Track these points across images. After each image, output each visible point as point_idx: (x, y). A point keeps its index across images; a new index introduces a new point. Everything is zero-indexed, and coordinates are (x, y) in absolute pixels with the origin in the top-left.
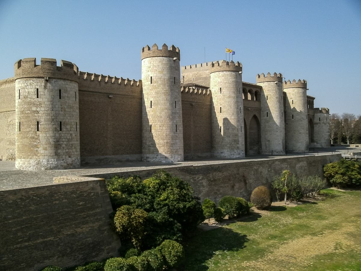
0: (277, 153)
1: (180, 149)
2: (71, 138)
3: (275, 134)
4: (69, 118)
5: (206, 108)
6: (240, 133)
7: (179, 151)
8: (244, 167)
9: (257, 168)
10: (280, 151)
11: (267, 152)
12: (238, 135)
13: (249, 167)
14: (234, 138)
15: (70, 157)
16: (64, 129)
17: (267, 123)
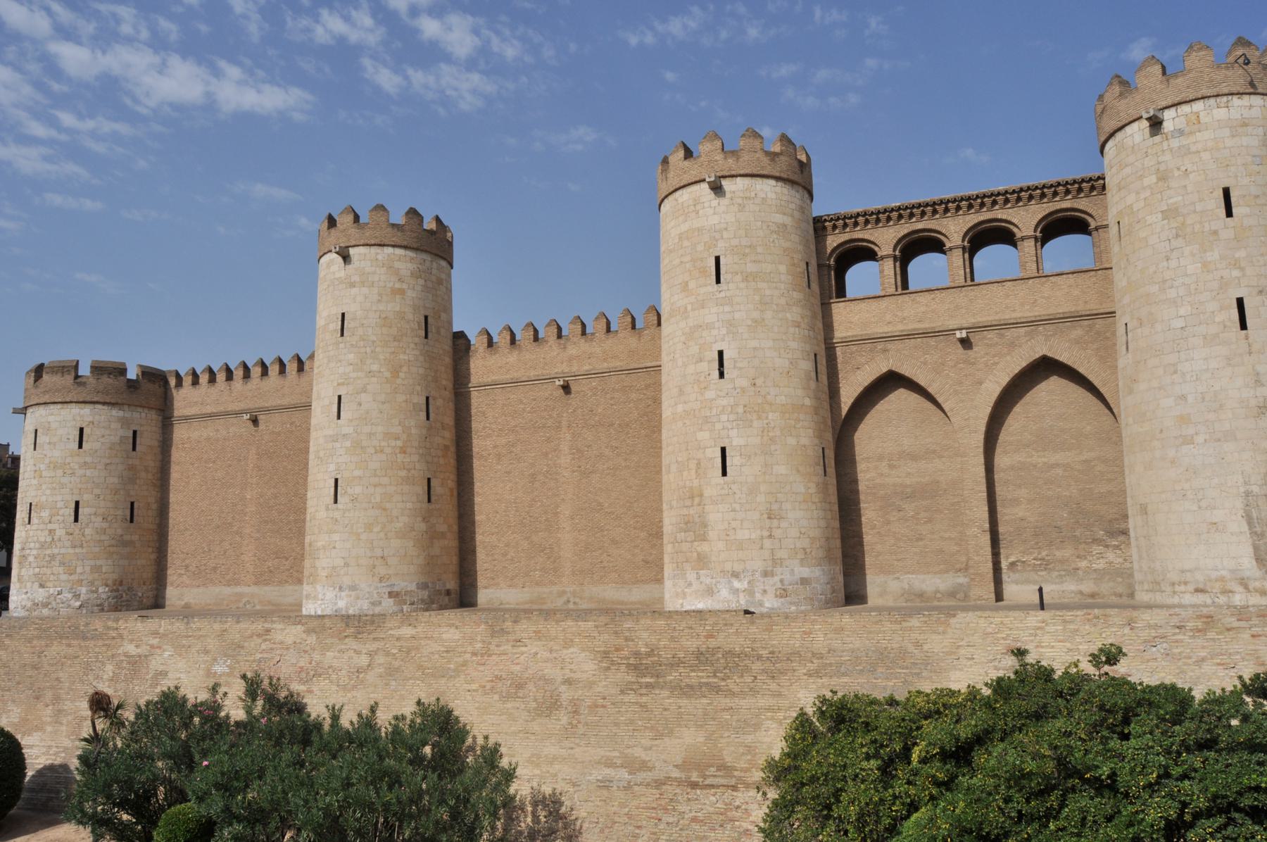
0: (1197, 590)
1: (346, 565)
2: (49, 539)
3: (1173, 462)
4: (48, 492)
5: (647, 386)
6: (722, 480)
7: (342, 572)
8: (75, 642)
9: (143, 650)
10: (1222, 579)
11: (1146, 587)
12: (701, 495)
13: (100, 643)
14: (685, 511)
15: (42, 586)
16: (34, 520)
17: (1131, 392)
